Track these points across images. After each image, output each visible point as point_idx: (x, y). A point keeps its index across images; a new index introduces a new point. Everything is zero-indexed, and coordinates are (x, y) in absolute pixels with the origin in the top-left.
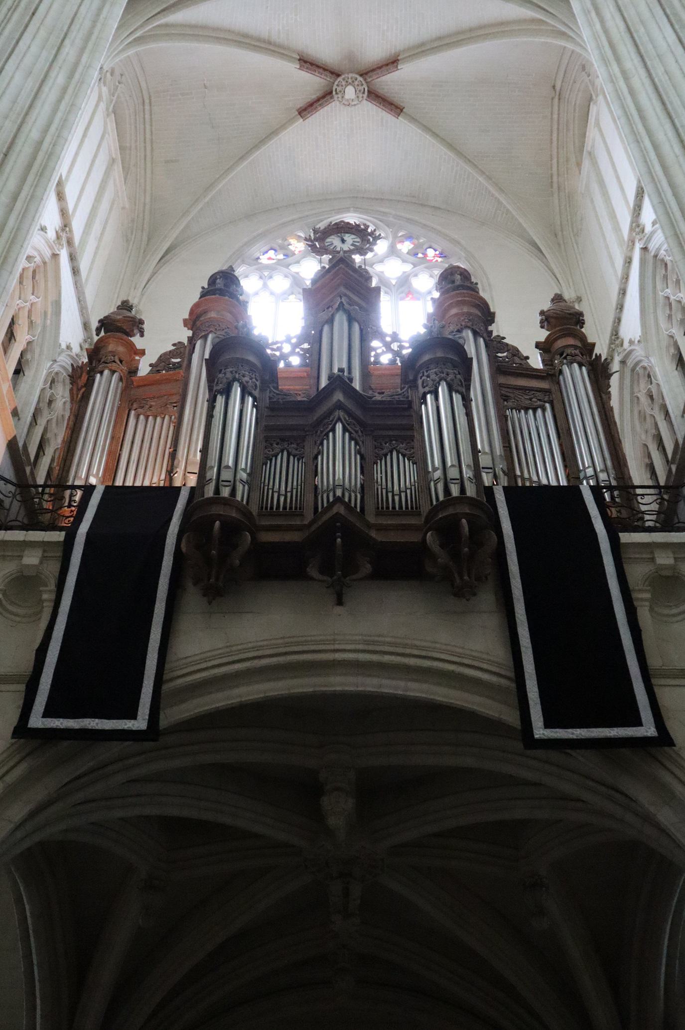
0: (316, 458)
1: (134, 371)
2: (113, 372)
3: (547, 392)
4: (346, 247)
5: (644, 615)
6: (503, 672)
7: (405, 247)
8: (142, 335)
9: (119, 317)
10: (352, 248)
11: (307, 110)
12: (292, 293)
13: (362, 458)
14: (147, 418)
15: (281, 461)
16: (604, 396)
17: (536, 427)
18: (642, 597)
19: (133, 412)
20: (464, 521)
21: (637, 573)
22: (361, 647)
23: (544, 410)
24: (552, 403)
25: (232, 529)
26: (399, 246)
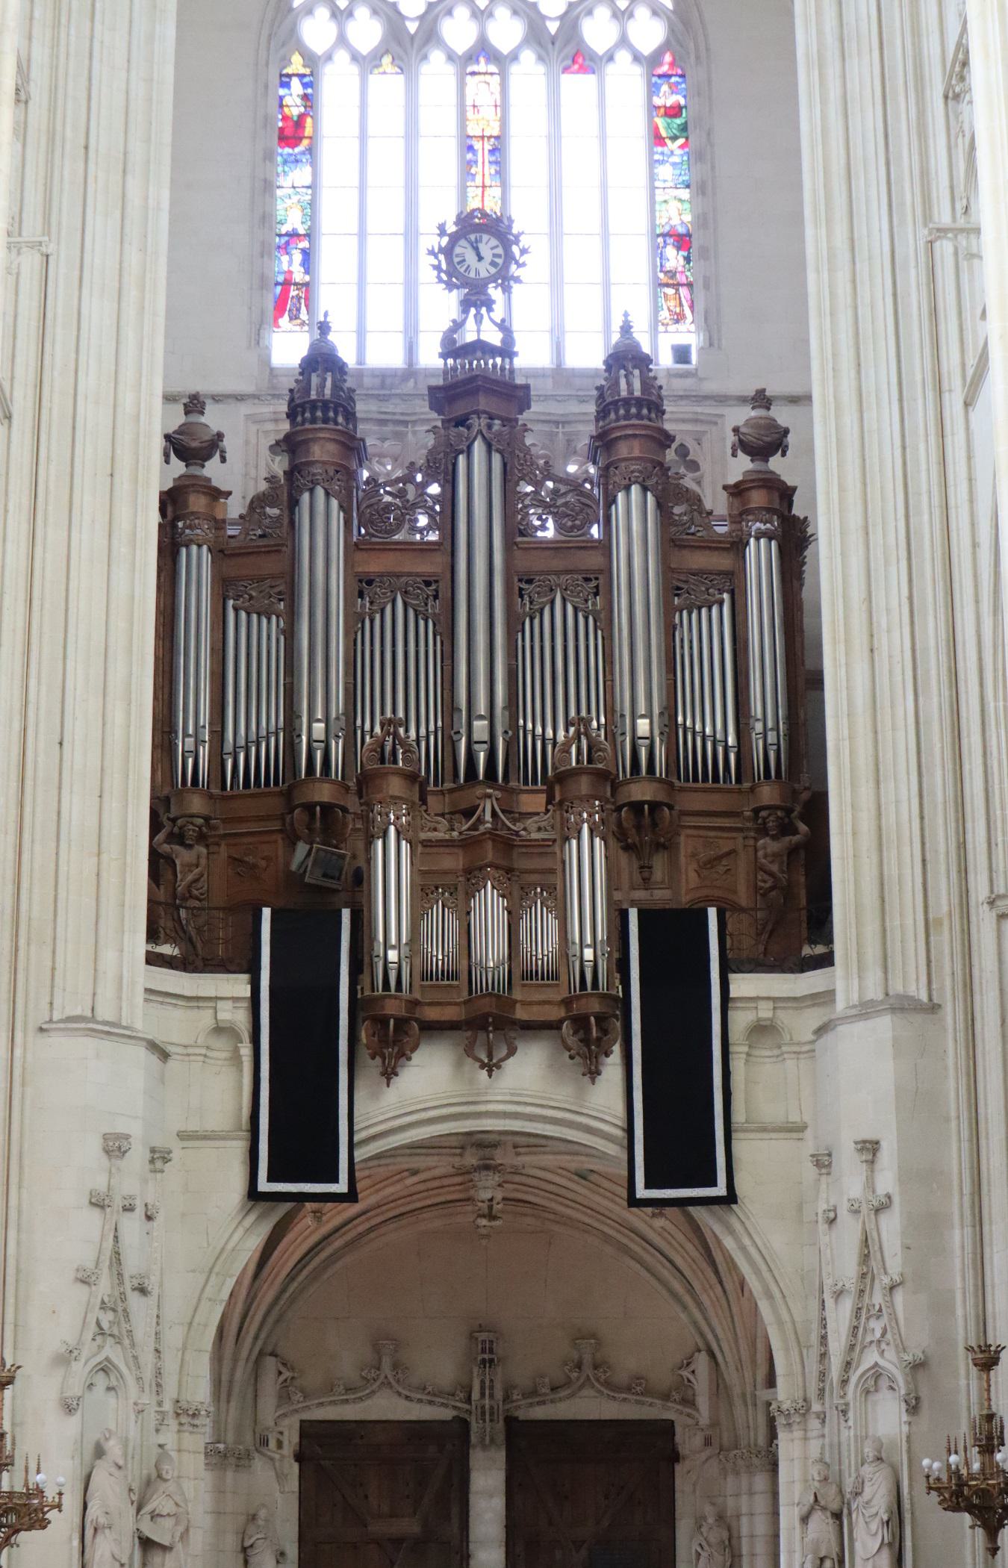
0: (469, 913)
1: (219, 524)
2: (200, 546)
3: (729, 574)
4: (484, 269)
5: (737, 1065)
6: (620, 1123)
8: (223, 460)
9: (195, 444)
10: (493, 270)
12: (387, 52)
13: (509, 913)
14: (248, 614)
15: (437, 910)
16: (795, 583)
17: (707, 630)
18: (738, 1049)
19: (231, 602)
20: (592, 1019)
21: (741, 1020)
22: (508, 1098)
23: (721, 603)
24: (732, 593)
25: (402, 1023)
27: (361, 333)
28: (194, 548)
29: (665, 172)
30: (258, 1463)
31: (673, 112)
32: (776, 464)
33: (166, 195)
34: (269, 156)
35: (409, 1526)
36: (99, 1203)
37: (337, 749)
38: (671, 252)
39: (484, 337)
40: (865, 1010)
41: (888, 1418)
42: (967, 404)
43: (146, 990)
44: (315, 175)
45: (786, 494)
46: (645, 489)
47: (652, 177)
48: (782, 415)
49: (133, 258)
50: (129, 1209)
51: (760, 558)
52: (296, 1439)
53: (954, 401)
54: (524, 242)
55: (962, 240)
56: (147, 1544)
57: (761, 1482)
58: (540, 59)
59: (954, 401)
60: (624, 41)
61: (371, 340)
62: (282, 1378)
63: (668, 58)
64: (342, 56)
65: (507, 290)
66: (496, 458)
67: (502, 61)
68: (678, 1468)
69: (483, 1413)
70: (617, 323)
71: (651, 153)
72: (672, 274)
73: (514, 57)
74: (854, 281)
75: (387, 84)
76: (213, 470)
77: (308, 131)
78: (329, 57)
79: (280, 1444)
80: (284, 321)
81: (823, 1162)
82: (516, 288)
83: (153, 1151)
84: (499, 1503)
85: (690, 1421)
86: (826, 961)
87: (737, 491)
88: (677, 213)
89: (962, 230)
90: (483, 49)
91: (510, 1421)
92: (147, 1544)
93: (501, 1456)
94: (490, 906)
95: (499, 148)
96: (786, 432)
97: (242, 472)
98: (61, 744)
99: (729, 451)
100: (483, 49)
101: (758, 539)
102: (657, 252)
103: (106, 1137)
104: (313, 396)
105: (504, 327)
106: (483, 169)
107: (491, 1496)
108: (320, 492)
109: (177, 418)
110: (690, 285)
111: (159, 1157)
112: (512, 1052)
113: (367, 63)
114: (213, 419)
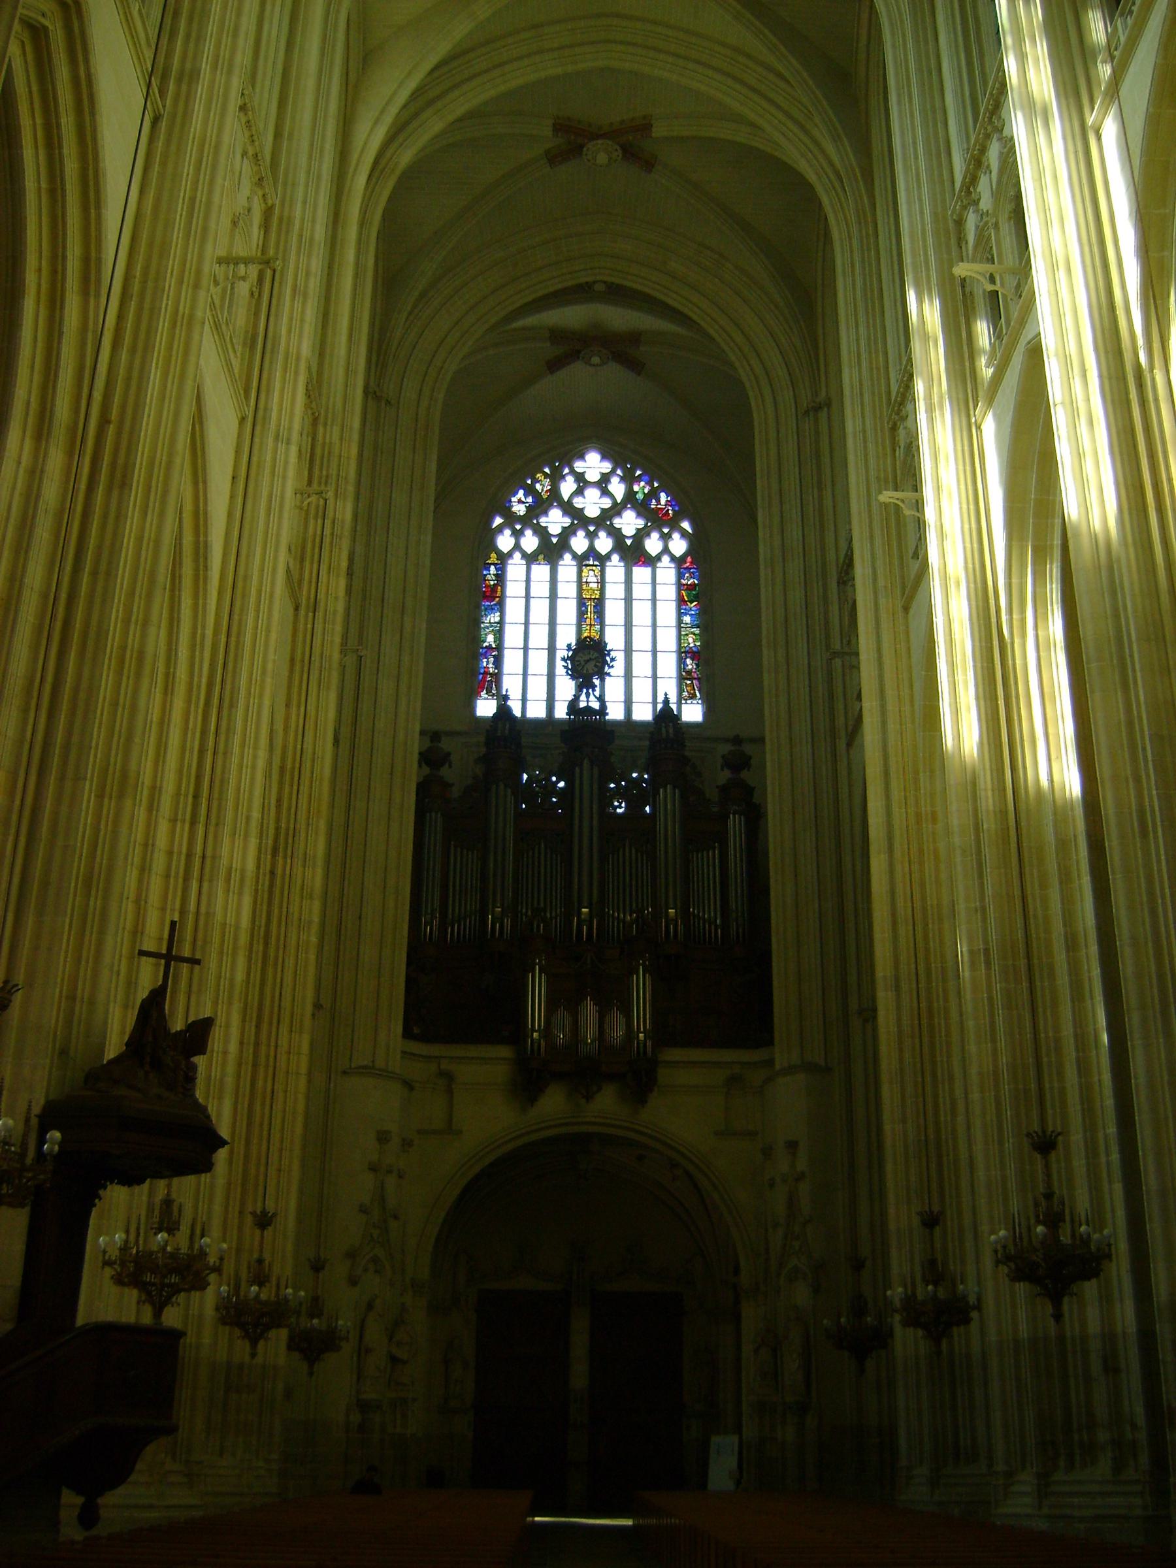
7: (641, 488)
8: (450, 766)
11: (554, 365)
26: (636, 488)
27: (524, 700)
28: (433, 814)
29: (687, 619)
31: (690, 588)
32: (744, 774)
33: (424, 626)
34: (478, 606)
36: (373, 1168)
37: (507, 922)
38: (689, 661)
39: (590, 704)
40: (789, 1070)
41: (802, 1295)
42: (849, 745)
43: (404, 1052)
44: (502, 616)
45: (749, 791)
46: (674, 787)
47: (680, 621)
48: (748, 749)
49: (406, 658)
50: (390, 1172)
51: (735, 824)
53: (842, 744)
54: (613, 654)
55: (847, 658)
56: (394, 1359)
58: (622, 559)
59: (842, 744)
60: (666, 550)
61: (529, 704)
63: (689, 559)
64: (517, 556)
65: (602, 681)
66: (596, 771)
67: (603, 560)
70: (660, 698)
71: (679, 609)
72: (689, 672)
73: (608, 557)
74: (788, 679)
75: (541, 571)
76: (445, 772)
77: (499, 594)
78: (510, 554)
80: (484, 694)
81: (767, 1152)
82: (607, 678)
83: (404, 1140)
86: (771, 1043)
87: (723, 789)
88: (691, 642)
89: (847, 654)
90: (592, 552)
92: (394, 1359)
94: (589, 1010)
95: (600, 604)
96: (750, 758)
97: (459, 773)
98: (360, 918)
99: (719, 768)
100: (592, 552)
101: (734, 814)
102: (681, 662)
103: (378, 1132)
104: (499, 734)
105: (601, 699)
106: (590, 615)
108: (502, 786)
109: (428, 744)
110: (698, 679)
111: (406, 1144)
112: (600, 1089)
113: (530, 559)
114: (446, 744)
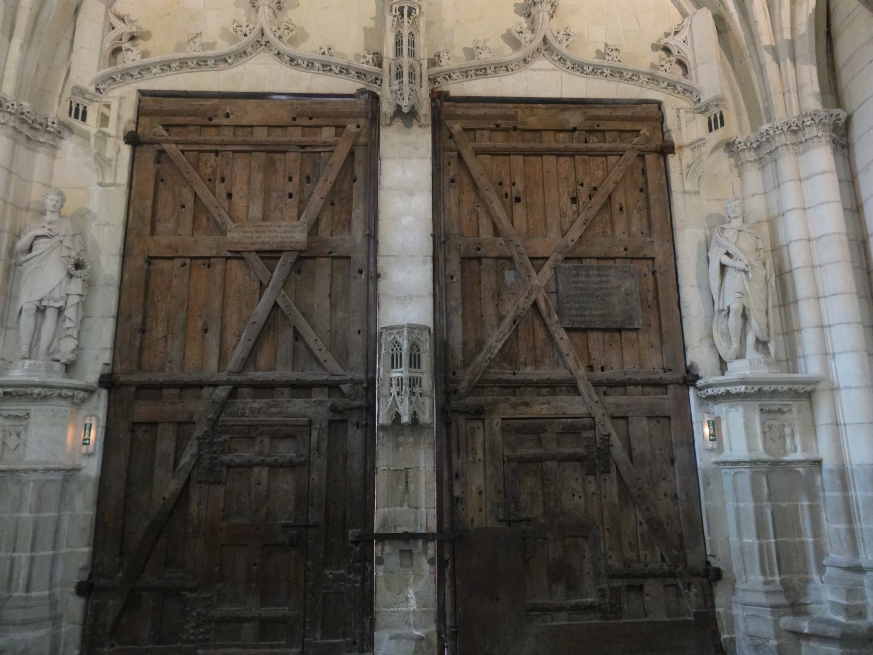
30: (69, 145)
35: (291, 232)
52: (129, 113)
57: (821, 157)
62: (113, 34)
68: (673, 161)
69: (399, 75)
79: (104, 120)
84: (423, 203)
85: (684, 103)
91: (439, 98)
93: (422, 139)
107: (411, 193)
